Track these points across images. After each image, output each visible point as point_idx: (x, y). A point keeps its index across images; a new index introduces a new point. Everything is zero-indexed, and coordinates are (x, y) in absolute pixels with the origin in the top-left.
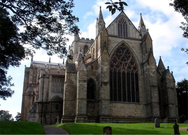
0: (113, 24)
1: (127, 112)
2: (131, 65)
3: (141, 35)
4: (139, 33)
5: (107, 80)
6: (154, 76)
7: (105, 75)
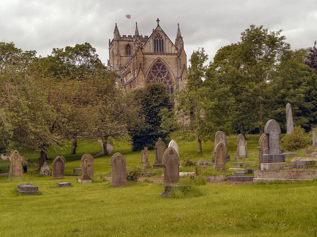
3: (177, 49)
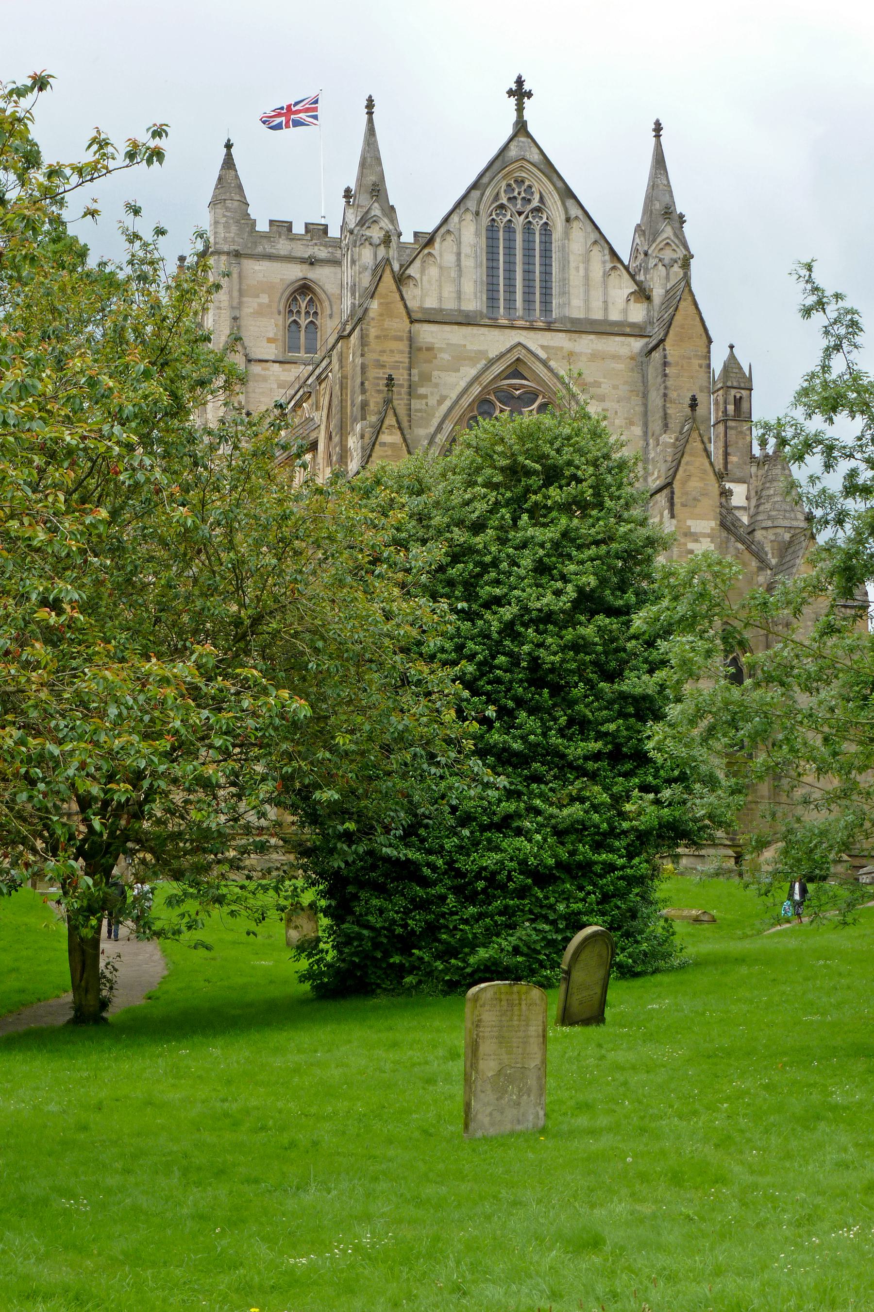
0: (448, 232)
3: (643, 294)
4: (633, 277)
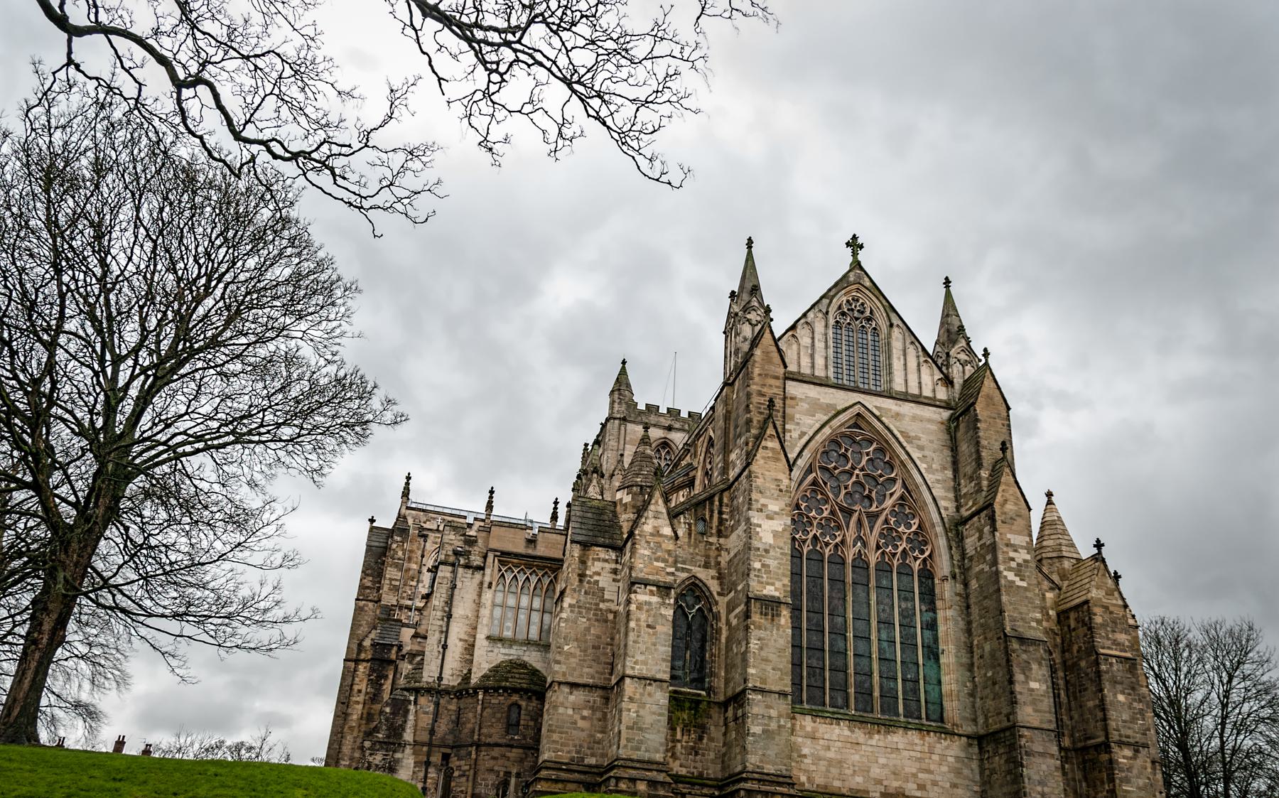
1: (876, 772)
2: (898, 523)
4: (940, 369)
5: (775, 588)
6: (1024, 584)
7: (768, 561)
